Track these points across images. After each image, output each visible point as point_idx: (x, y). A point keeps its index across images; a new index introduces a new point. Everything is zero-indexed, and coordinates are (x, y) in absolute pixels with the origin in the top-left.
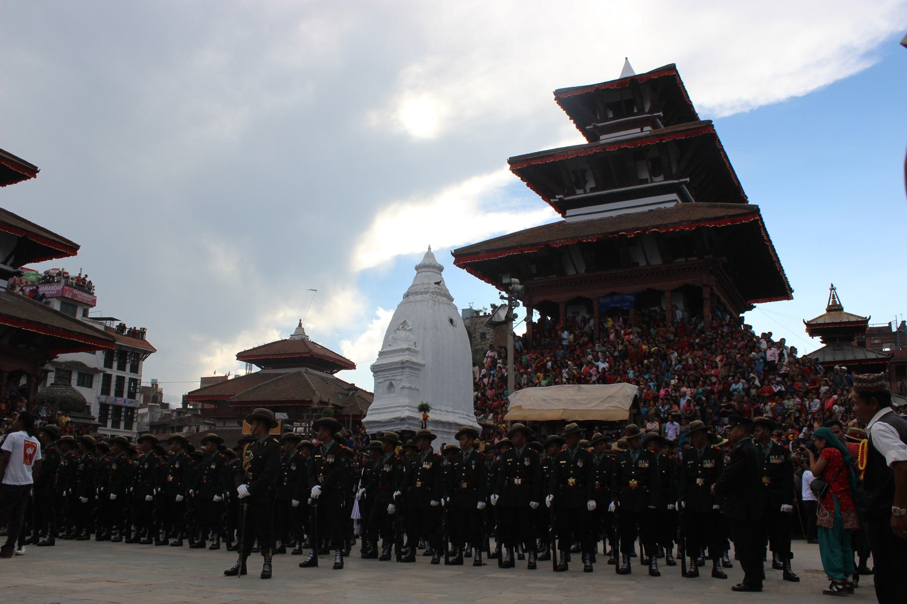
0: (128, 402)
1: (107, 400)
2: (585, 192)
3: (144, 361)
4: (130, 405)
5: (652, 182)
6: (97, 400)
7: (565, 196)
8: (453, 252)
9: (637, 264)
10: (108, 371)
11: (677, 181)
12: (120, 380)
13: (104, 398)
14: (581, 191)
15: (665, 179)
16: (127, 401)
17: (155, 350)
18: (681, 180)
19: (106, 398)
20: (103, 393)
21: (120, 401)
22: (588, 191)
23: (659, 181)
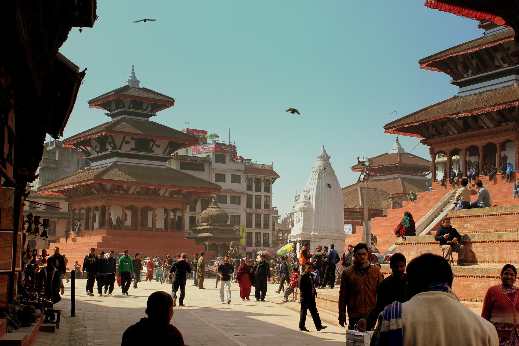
0: (265, 211)
1: (251, 211)
2: (468, 76)
3: (273, 184)
4: (266, 213)
5: (503, 68)
6: (244, 212)
7: (457, 80)
8: (384, 126)
9: (482, 127)
10: (250, 193)
11: (514, 67)
12: (258, 198)
13: (248, 210)
14: (465, 76)
15: (509, 66)
16: (264, 210)
17: (279, 176)
18: (516, 66)
19: (250, 210)
20: (247, 207)
21: (259, 211)
22: (470, 75)
23: (506, 67)
